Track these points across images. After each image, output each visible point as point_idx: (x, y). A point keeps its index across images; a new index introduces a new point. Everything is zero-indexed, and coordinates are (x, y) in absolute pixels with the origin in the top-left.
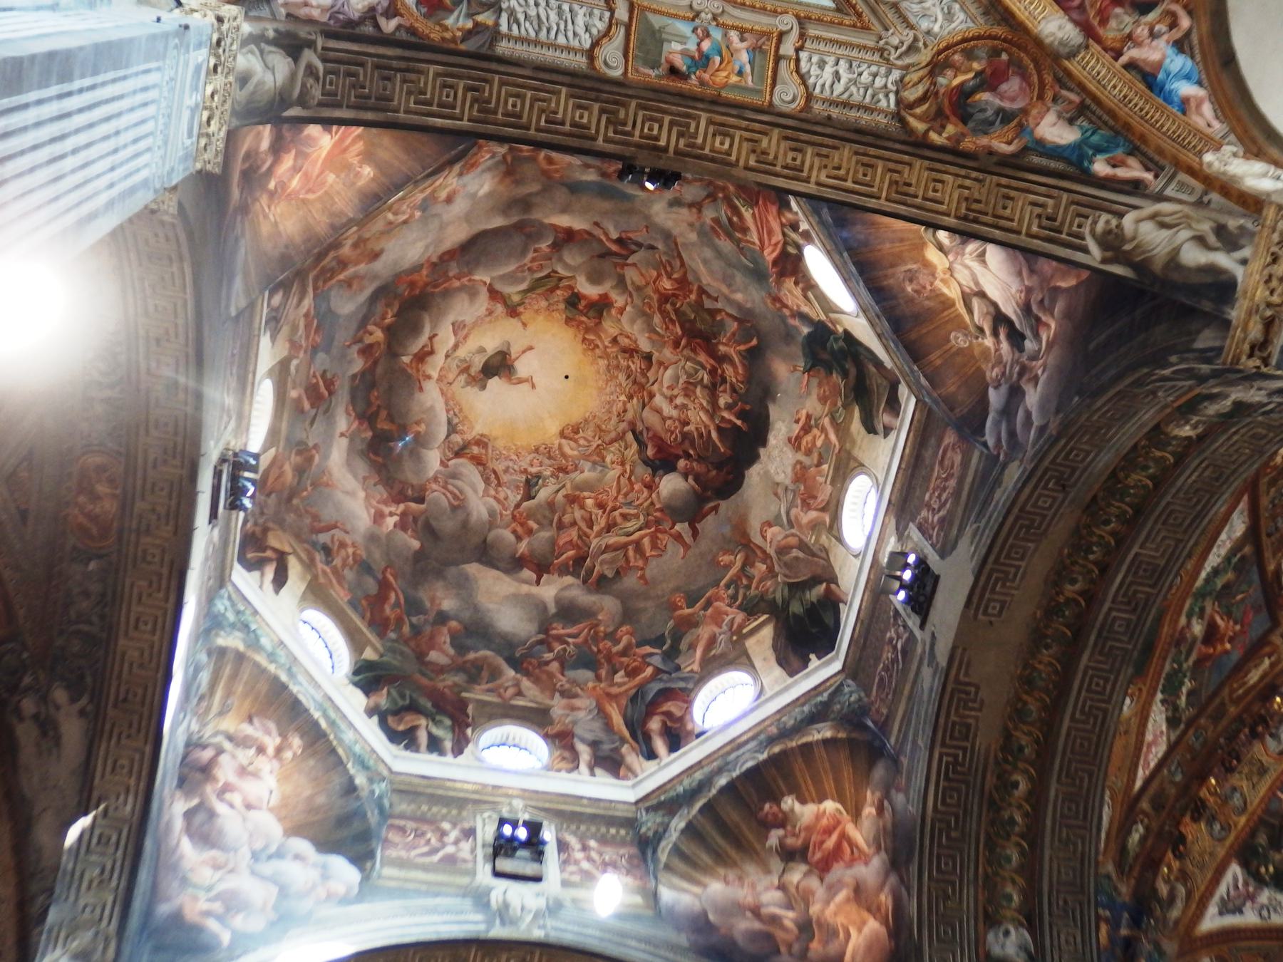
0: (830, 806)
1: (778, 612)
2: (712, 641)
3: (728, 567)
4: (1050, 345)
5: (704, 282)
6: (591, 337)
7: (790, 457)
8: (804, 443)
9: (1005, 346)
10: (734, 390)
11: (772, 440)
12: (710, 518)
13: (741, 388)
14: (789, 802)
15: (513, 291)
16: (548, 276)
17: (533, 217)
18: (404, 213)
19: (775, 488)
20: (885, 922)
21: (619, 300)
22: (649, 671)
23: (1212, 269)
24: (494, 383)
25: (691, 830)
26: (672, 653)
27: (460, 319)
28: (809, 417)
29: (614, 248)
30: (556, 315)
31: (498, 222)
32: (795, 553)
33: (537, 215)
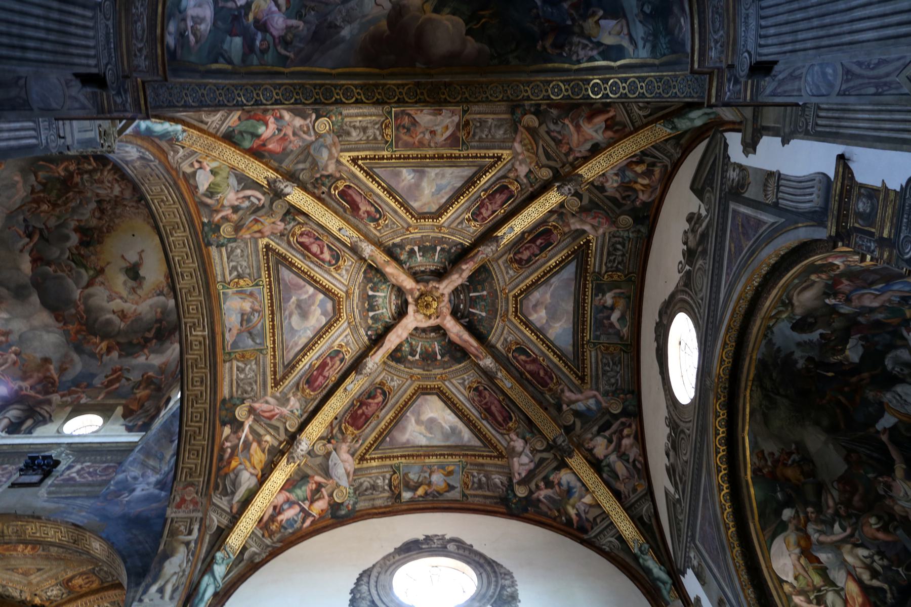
5: (25, 194)
6: (105, 230)
15: (85, 276)
16: (73, 261)
17: (29, 282)
18: (7, 359)
21: (73, 224)
24: (142, 273)
27: (106, 298)
29: (36, 238)
30: (98, 249)
31: (35, 298)
33: (27, 281)
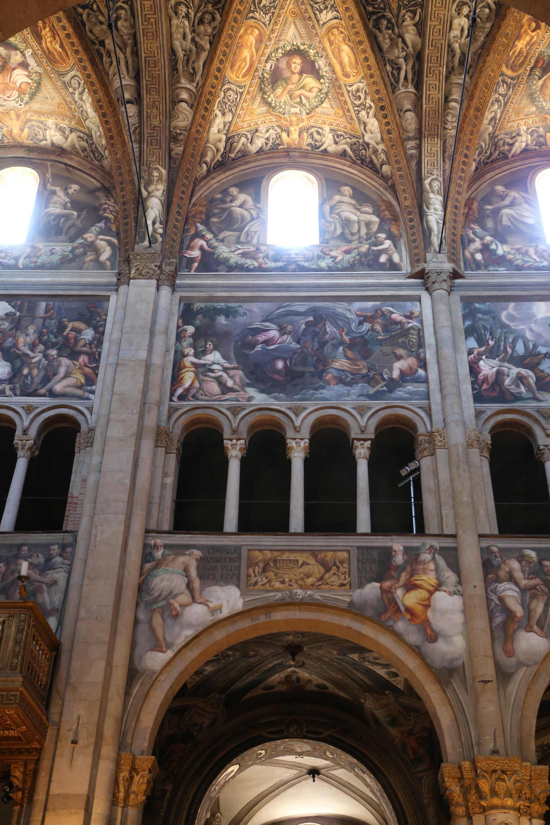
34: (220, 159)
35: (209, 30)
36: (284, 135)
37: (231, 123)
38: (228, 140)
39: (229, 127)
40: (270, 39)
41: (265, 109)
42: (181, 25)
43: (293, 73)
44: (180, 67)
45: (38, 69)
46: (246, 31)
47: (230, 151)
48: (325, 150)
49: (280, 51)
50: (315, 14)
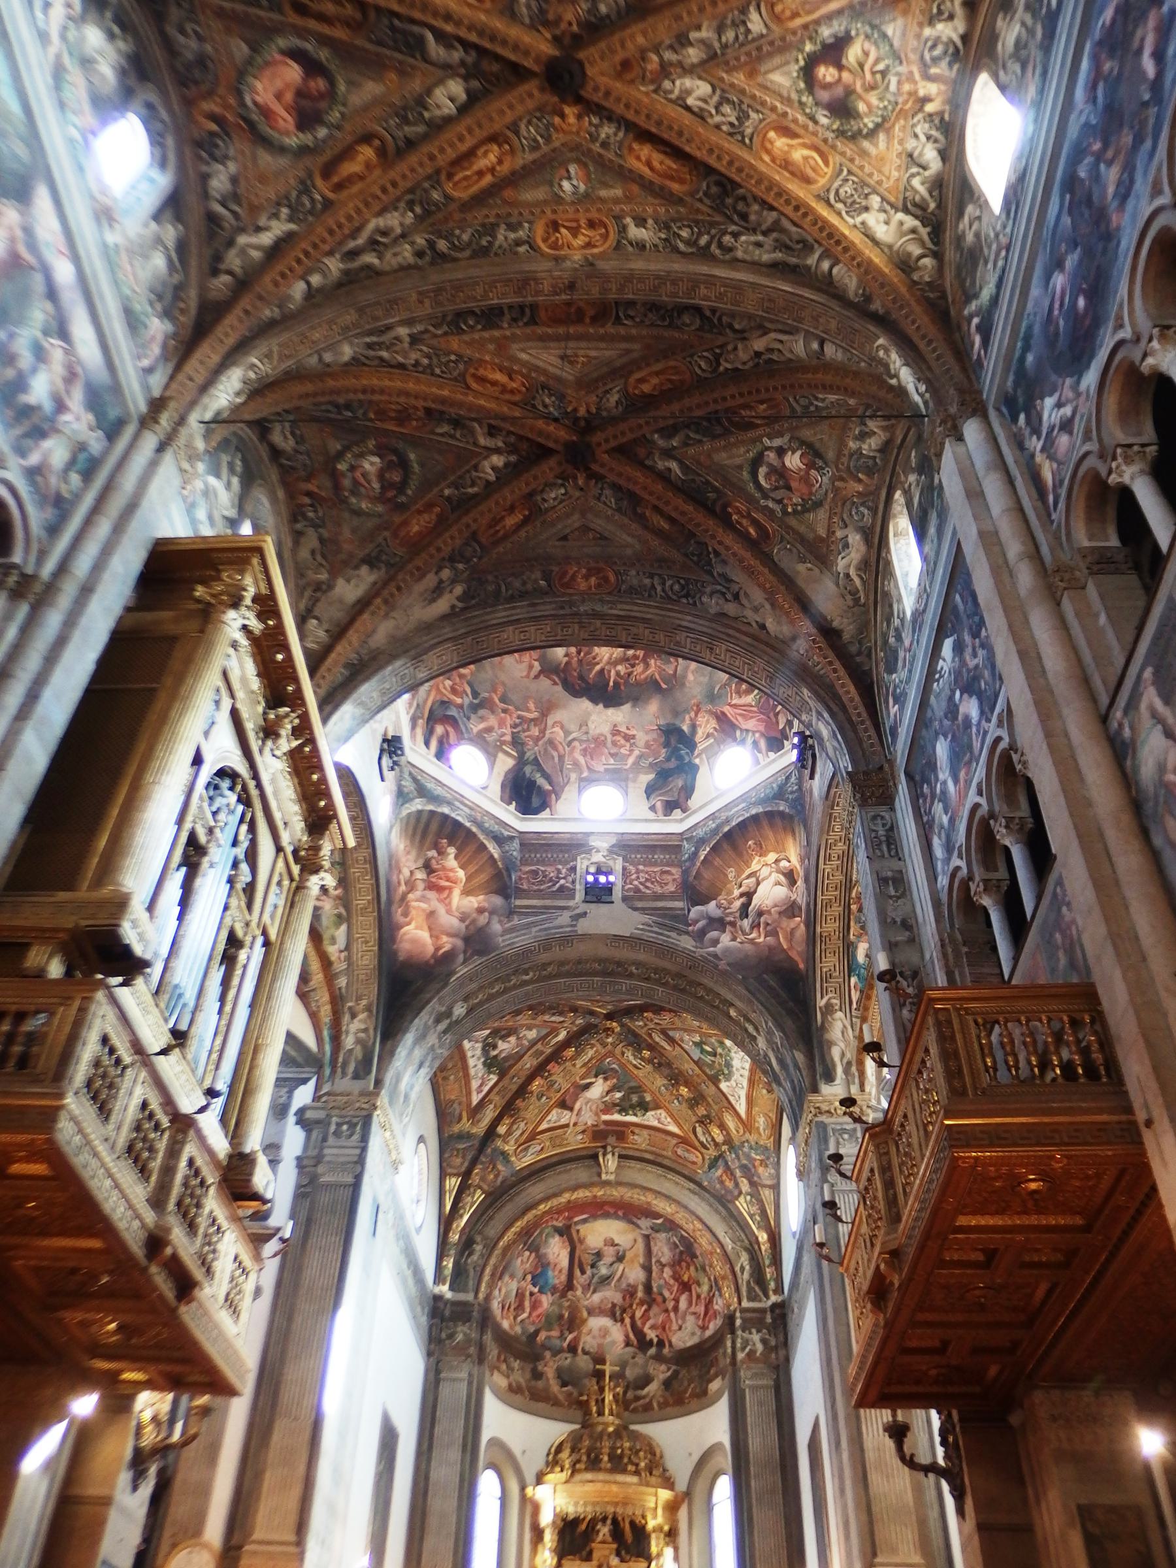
0: (461, 874)
1: (521, 762)
2: (489, 730)
3: (528, 710)
4: (752, 941)
7: (605, 729)
8: (618, 738)
9: (738, 904)
10: (629, 674)
11: (611, 711)
12: (548, 682)
13: (632, 680)
14: (452, 851)
19: (583, 724)
20: (437, 949)
22: (459, 701)
23: (834, 1066)
25: (420, 812)
26: (475, 708)
28: (634, 737)
32: (555, 754)
34: (928, 229)
35: (756, 207)
36: (930, 108)
37: (883, 199)
38: (906, 211)
39: (889, 203)
40: (785, 114)
41: (882, 137)
42: (744, 245)
43: (840, 80)
44: (793, 260)
45: (786, 438)
46: (768, 152)
47: (924, 209)
48: (965, 38)
49: (804, 99)
50: (754, 40)
